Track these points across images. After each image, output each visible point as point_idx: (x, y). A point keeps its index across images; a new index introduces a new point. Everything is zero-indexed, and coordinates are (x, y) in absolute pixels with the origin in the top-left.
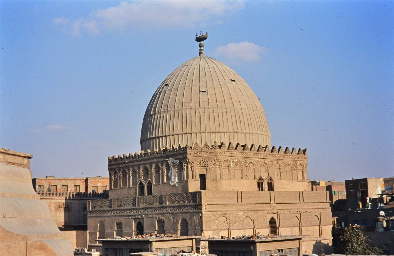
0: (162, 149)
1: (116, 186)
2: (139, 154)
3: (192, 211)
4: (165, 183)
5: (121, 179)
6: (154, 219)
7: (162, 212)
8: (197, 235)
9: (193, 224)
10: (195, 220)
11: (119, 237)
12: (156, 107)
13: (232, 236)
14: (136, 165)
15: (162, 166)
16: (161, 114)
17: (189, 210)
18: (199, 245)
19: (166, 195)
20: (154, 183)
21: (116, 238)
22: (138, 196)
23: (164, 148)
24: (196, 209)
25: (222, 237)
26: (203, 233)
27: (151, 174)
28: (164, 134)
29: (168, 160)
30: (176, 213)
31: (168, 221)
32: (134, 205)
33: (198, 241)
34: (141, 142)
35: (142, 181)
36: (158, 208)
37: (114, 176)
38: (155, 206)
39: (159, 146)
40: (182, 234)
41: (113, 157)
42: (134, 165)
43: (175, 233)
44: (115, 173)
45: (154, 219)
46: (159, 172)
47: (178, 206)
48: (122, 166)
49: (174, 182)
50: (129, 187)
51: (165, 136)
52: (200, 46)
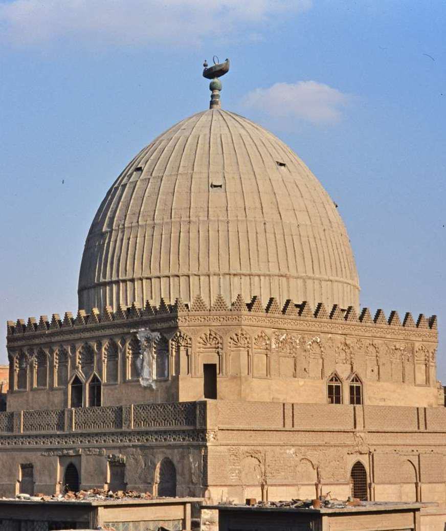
0: (124, 308)
1: (22, 384)
2: (75, 317)
3: (185, 443)
4: (129, 381)
5: (35, 371)
6: (103, 459)
7: (120, 444)
8: (194, 496)
9: (186, 472)
10: (190, 463)
11: (27, 496)
12: (114, 217)
13: (271, 499)
14: (68, 341)
15: (123, 343)
16: (123, 232)
17: (180, 441)
18: (199, 517)
19: (130, 408)
20: (104, 380)
21: (19, 497)
22: (69, 407)
23: (130, 306)
24: (193, 439)
25: (248, 502)
26: (207, 492)
27: (100, 361)
28: (129, 276)
29: (137, 333)
30: (151, 447)
31: (133, 462)
32: (60, 426)
33: (197, 509)
34: (80, 292)
35: (80, 376)
36: (113, 434)
37: (20, 364)
38: (106, 430)
39: (117, 301)
40: (161, 493)
41: (18, 322)
42: (63, 341)
43: (148, 490)
44: (22, 357)
45: (103, 459)
46: (117, 356)
47: (156, 432)
48: (37, 341)
49: (147, 380)
50: (52, 388)
51: (132, 280)
52: (212, 88)
